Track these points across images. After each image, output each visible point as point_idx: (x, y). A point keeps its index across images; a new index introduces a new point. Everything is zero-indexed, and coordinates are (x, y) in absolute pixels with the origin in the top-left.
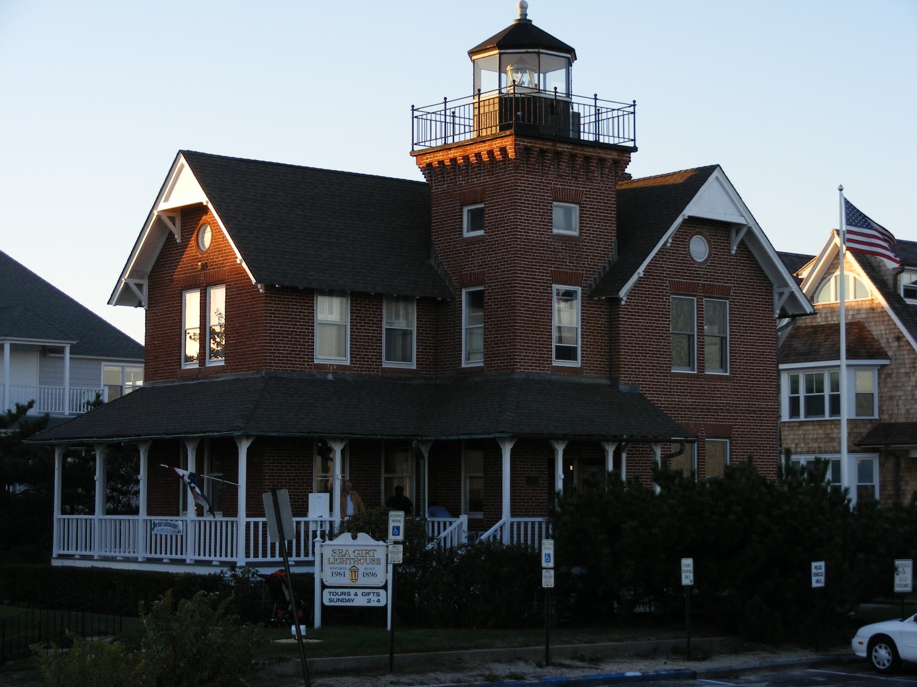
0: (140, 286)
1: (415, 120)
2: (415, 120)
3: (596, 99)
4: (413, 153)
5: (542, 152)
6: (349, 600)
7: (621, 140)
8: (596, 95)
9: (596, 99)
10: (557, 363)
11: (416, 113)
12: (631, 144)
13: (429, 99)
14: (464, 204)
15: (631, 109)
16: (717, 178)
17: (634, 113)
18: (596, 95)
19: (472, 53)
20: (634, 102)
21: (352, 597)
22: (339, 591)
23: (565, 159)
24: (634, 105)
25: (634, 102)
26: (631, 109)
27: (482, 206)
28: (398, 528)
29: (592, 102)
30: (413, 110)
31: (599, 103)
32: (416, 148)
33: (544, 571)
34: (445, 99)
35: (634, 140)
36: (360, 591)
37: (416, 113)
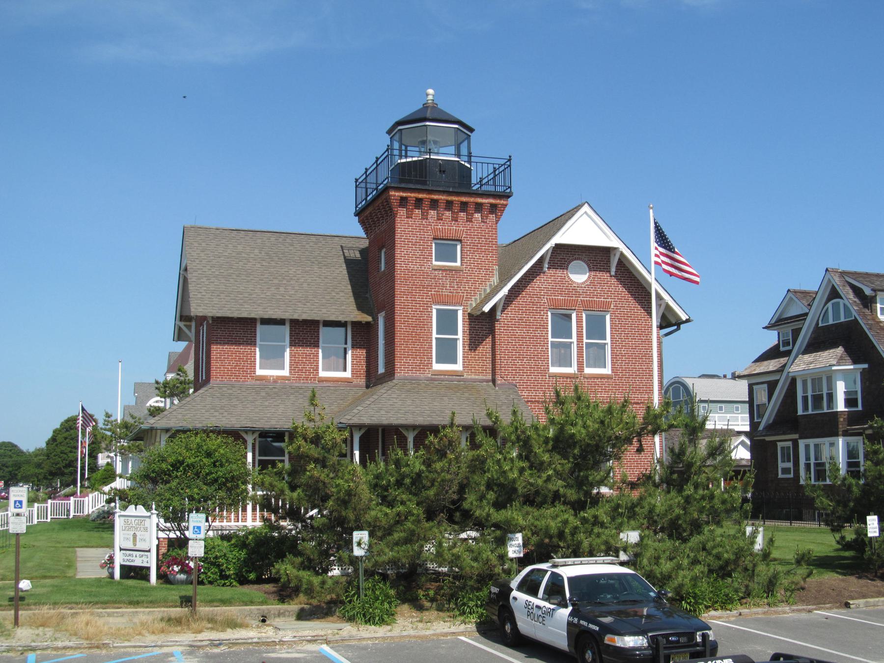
0: (189, 327)
4: (356, 215)
5: (419, 201)
6: (132, 561)
10: (437, 367)
16: (586, 213)
17: (510, 166)
21: (134, 558)
22: (128, 552)
24: (510, 160)
28: (21, 502)
33: (190, 542)
35: (510, 187)
36: (138, 553)
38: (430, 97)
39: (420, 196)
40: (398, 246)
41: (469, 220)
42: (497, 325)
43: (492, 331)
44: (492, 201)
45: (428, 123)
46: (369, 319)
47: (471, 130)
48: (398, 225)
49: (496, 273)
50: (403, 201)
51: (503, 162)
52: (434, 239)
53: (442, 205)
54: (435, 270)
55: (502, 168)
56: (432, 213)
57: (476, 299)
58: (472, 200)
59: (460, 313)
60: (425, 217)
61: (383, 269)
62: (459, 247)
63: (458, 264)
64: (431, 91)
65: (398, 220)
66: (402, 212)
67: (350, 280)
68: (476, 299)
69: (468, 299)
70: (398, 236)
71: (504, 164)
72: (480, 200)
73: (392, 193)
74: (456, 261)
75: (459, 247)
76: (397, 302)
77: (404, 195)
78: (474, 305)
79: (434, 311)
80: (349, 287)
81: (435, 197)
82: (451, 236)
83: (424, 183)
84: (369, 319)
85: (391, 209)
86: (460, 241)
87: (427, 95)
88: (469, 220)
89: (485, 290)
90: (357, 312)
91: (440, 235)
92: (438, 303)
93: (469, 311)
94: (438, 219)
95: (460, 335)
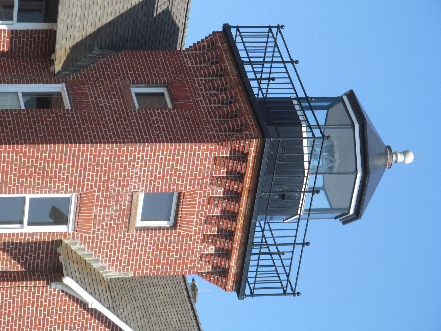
1: (267, 30)
2: (267, 30)
3: (303, 244)
4: (227, 27)
5: (240, 177)
7: (251, 281)
8: (308, 244)
9: (303, 244)
11: (274, 30)
12: (248, 292)
13: (295, 42)
14: (168, 86)
15: (289, 291)
17: (285, 293)
18: (308, 244)
19: (351, 95)
20: (298, 294)
23: (231, 206)
24: (294, 294)
25: (298, 294)
26: (289, 291)
27: (170, 106)
29: (300, 240)
30: (279, 28)
31: (298, 248)
32: (233, 31)
34: (297, 62)
35: (252, 294)
37: (274, 30)
38: (401, 158)
39: (247, 180)
40: (172, 147)
41: (205, 239)
42: (41, 283)
43: (30, 274)
44: (233, 271)
45: (359, 175)
46: (58, 67)
47: (344, 223)
48: (204, 146)
49: (122, 275)
50: (243, 157)
51: (292, 278)
52: (180, 194)
53: (231, 206)
54: (132, 196)
55: (281, 270)
56: (220, 192)
57: (83, 249)
58: (236, 245)
59: (61, 228)
60: (214, 181)
61: (137, 107)
62: (164, 223)
63: (140, 223)
64: (410, 158)
65: (212, 146)
66: (225, 152)
67: (122, 15)
68: (83, 249)
69: (84, 239)
70: (187, 146)
71: (288, 281)
72: (235, 256)
73: (255, 143)
74: (143, 219)
75: (164, 223)
76: (83, 147)
77: (251, 159)
78: (74, 248)
79: (68, 195)
80: (110, 19)
81: (244, 199)
82: (184, 216)
83: (271, 171)
84: (58, 67)
85: (227, 139)
86: (174, 226)
87: (405, 153)
88: (208, 221)
89: (97, 261)
90: (70, 45)
91: (185, 201)
92: (79, 200)
93: (65, 241)
94: (209, 199)
95: (28, 229)
